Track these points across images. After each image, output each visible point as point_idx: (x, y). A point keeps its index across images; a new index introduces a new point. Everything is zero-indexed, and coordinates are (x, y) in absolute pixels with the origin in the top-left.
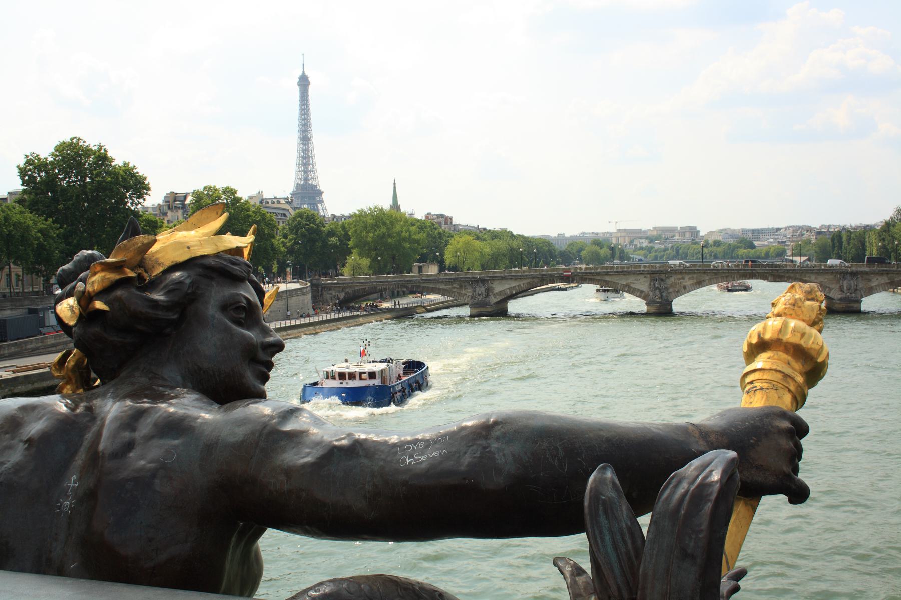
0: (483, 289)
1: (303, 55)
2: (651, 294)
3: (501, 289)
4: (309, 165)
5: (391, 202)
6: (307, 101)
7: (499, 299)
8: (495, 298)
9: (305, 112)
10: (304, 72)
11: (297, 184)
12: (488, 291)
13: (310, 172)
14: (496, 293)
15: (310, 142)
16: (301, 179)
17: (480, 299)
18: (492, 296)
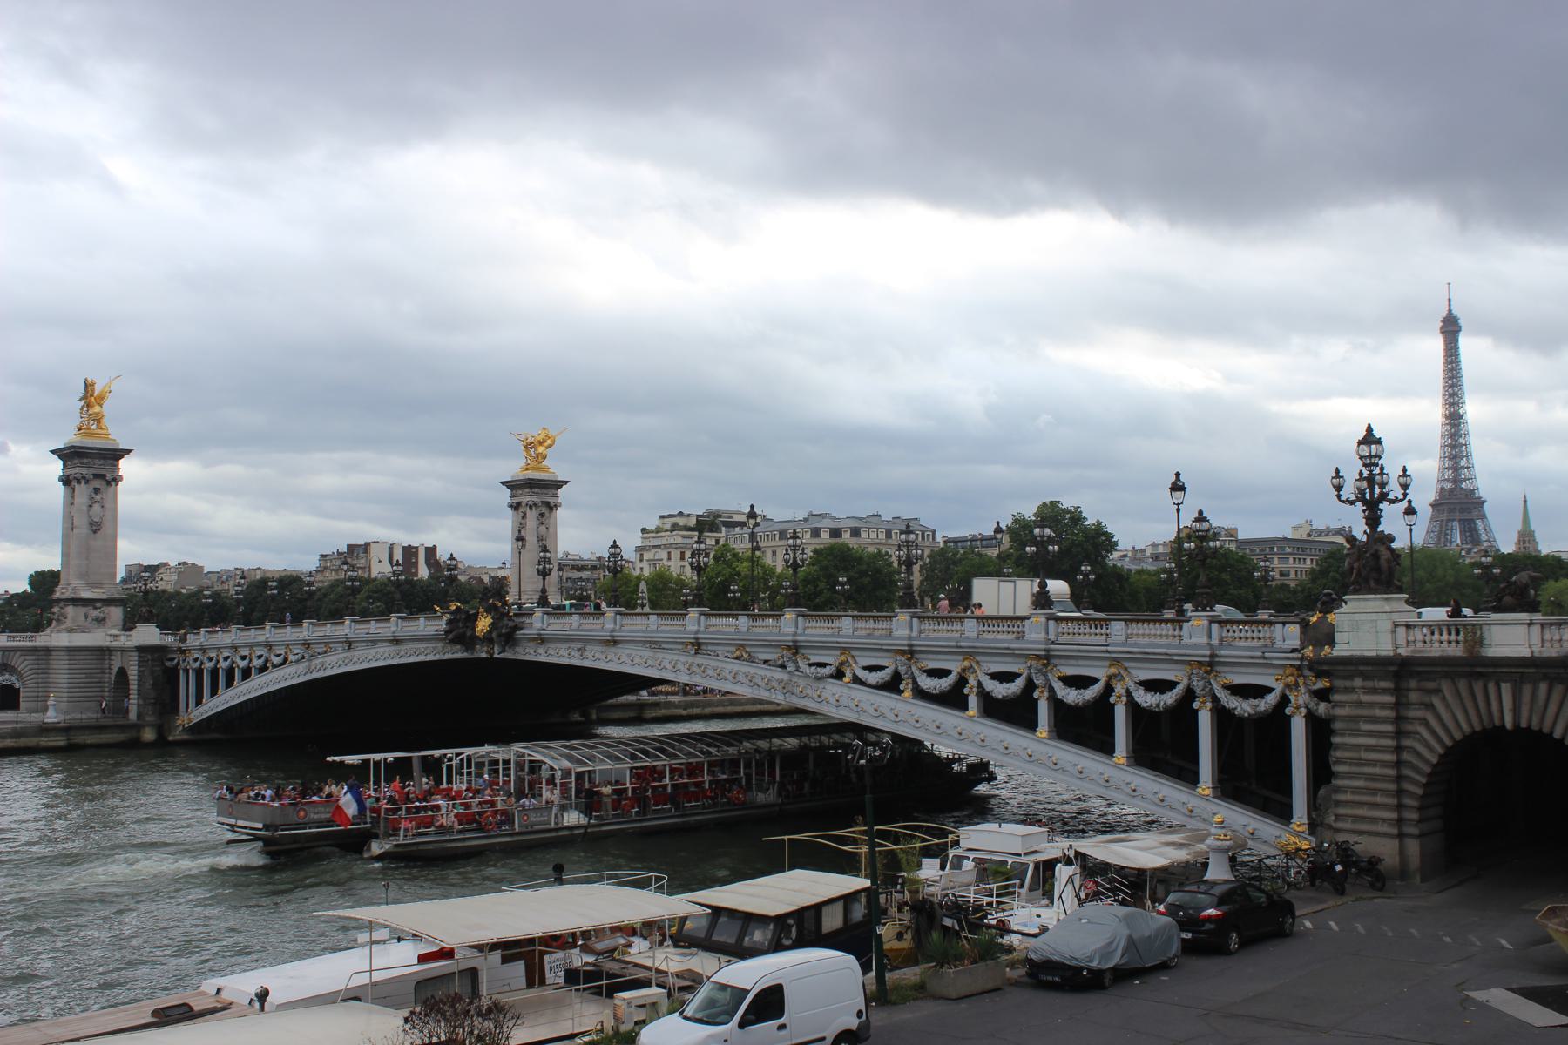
4: (1462, 458)
5: (1519, 527)
6: (1457, 356)
10: (1450, 310)
11: (1442, 489)
13: (1464, 468)
15: (1461, 421)
16: (1447, 480)
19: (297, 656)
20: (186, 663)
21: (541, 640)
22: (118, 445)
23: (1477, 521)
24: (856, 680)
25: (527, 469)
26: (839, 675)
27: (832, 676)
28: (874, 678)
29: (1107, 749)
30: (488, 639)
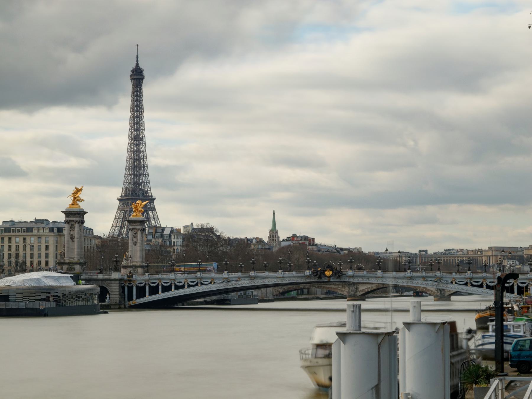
0: (354, 288)
1: (137, 45)
2: (436, 292)
3: (363, 289)
4: (140, 168)
5: (270, 228)
6: (141, 96)
7: (362, 293)
8: (360, 293)
9: (137, 109)
10: (137, 64)
11: (126, 189)
12: (357, 289)
14: (361, 291)
15: (142, 142)
17: (352, 293)
18: (358, 292)
19: (221, 282)
20: (132, 284)
21: (353, 277)
22: (83, 210)
23: (149, 212)
24: (456, 283)
25: (136, 216)
26: (452, 283)
27: (450, 283)
28: (461, 283)
29: (513, 293)
30: (330, 277)
